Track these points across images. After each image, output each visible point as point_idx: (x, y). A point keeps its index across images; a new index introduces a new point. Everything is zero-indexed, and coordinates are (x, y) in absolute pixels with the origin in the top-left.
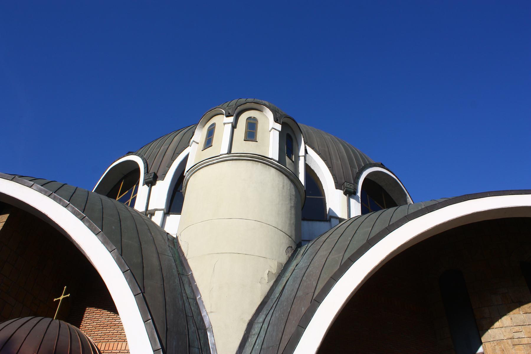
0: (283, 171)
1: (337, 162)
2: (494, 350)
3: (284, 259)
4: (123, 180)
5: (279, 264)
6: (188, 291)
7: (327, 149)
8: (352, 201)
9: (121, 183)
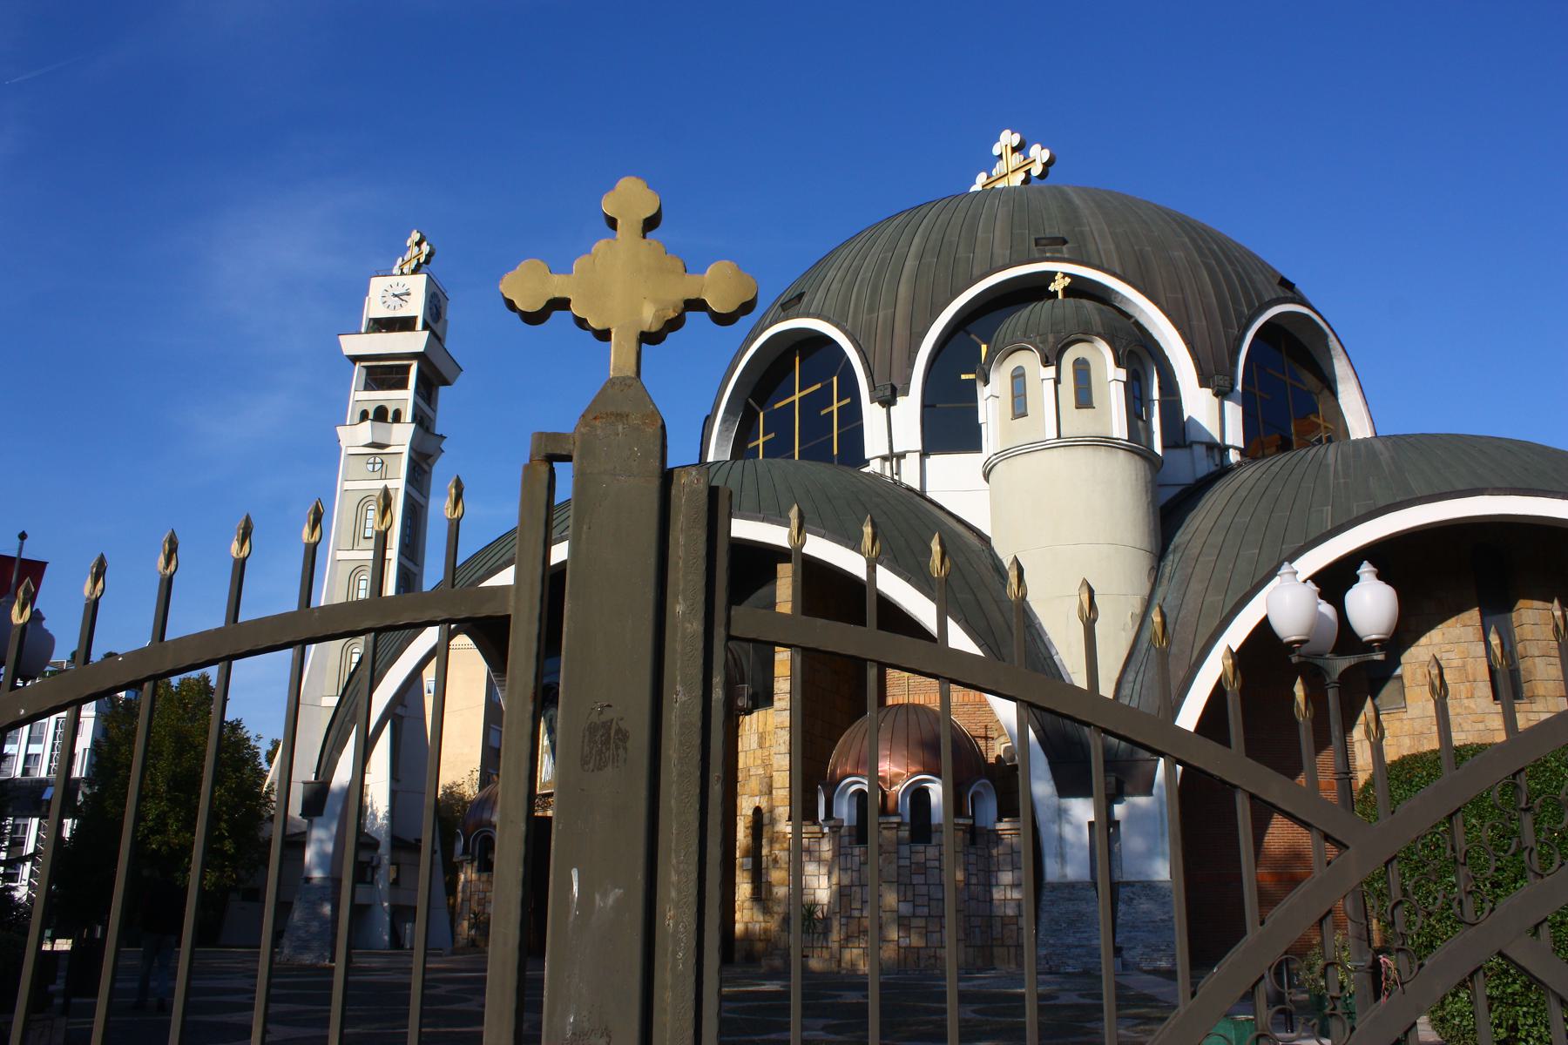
0: (1135, 450)
1: (1200, 324)
2: (1414, 673)
3: (1146, 591)
4: (797, 352)
5: (1143, 598)
6: (1043, 650)
7: (1180, 296)
8: (1228, 405)
9: (795, 361)
